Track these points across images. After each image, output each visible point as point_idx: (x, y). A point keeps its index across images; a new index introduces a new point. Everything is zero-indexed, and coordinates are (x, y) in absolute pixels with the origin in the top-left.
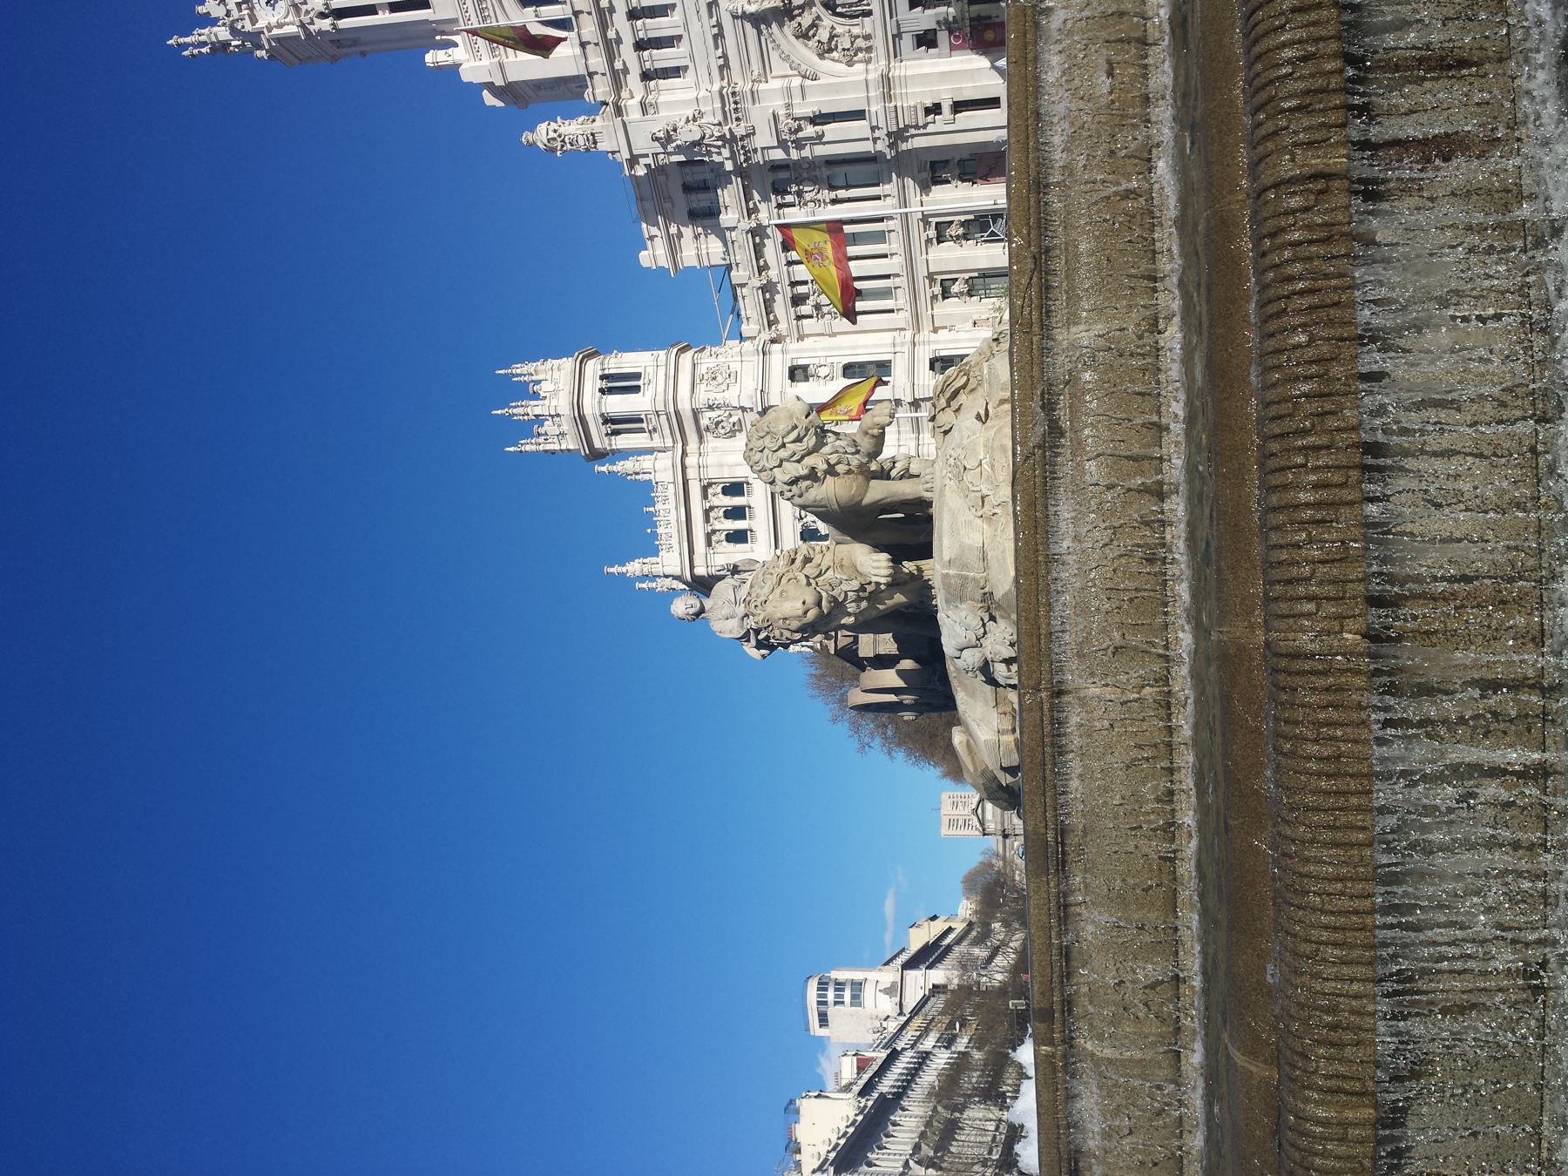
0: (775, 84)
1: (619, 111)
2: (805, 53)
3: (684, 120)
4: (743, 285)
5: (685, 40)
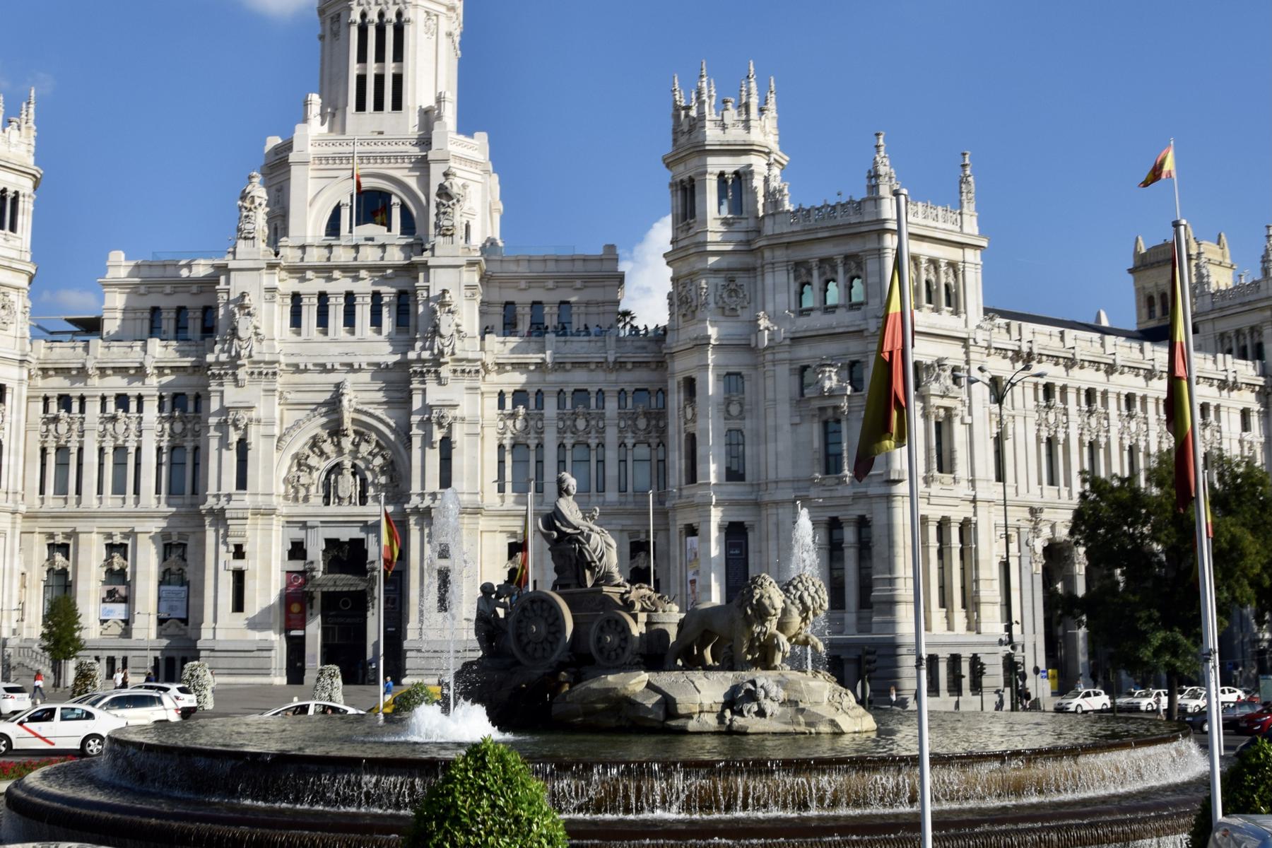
0: (277, 409)
1: (272, 266)
2: (299, 443)
3: (257, 324)
4: (86, 349)
5: (321, 337)
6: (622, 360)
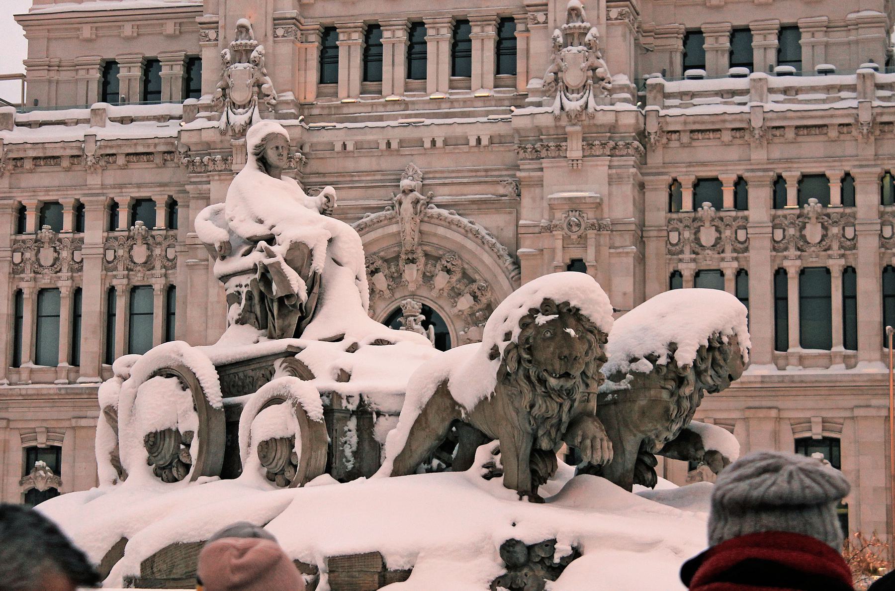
6: (885, 119)
